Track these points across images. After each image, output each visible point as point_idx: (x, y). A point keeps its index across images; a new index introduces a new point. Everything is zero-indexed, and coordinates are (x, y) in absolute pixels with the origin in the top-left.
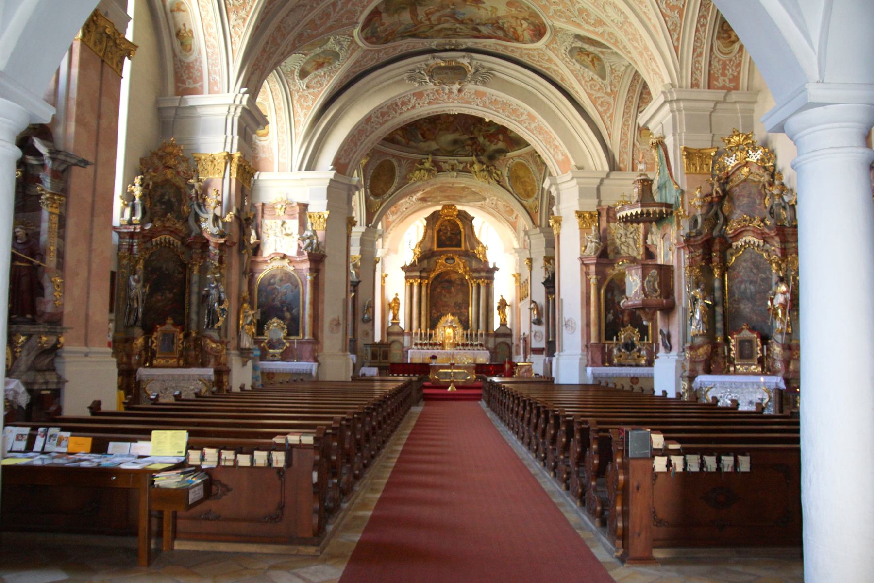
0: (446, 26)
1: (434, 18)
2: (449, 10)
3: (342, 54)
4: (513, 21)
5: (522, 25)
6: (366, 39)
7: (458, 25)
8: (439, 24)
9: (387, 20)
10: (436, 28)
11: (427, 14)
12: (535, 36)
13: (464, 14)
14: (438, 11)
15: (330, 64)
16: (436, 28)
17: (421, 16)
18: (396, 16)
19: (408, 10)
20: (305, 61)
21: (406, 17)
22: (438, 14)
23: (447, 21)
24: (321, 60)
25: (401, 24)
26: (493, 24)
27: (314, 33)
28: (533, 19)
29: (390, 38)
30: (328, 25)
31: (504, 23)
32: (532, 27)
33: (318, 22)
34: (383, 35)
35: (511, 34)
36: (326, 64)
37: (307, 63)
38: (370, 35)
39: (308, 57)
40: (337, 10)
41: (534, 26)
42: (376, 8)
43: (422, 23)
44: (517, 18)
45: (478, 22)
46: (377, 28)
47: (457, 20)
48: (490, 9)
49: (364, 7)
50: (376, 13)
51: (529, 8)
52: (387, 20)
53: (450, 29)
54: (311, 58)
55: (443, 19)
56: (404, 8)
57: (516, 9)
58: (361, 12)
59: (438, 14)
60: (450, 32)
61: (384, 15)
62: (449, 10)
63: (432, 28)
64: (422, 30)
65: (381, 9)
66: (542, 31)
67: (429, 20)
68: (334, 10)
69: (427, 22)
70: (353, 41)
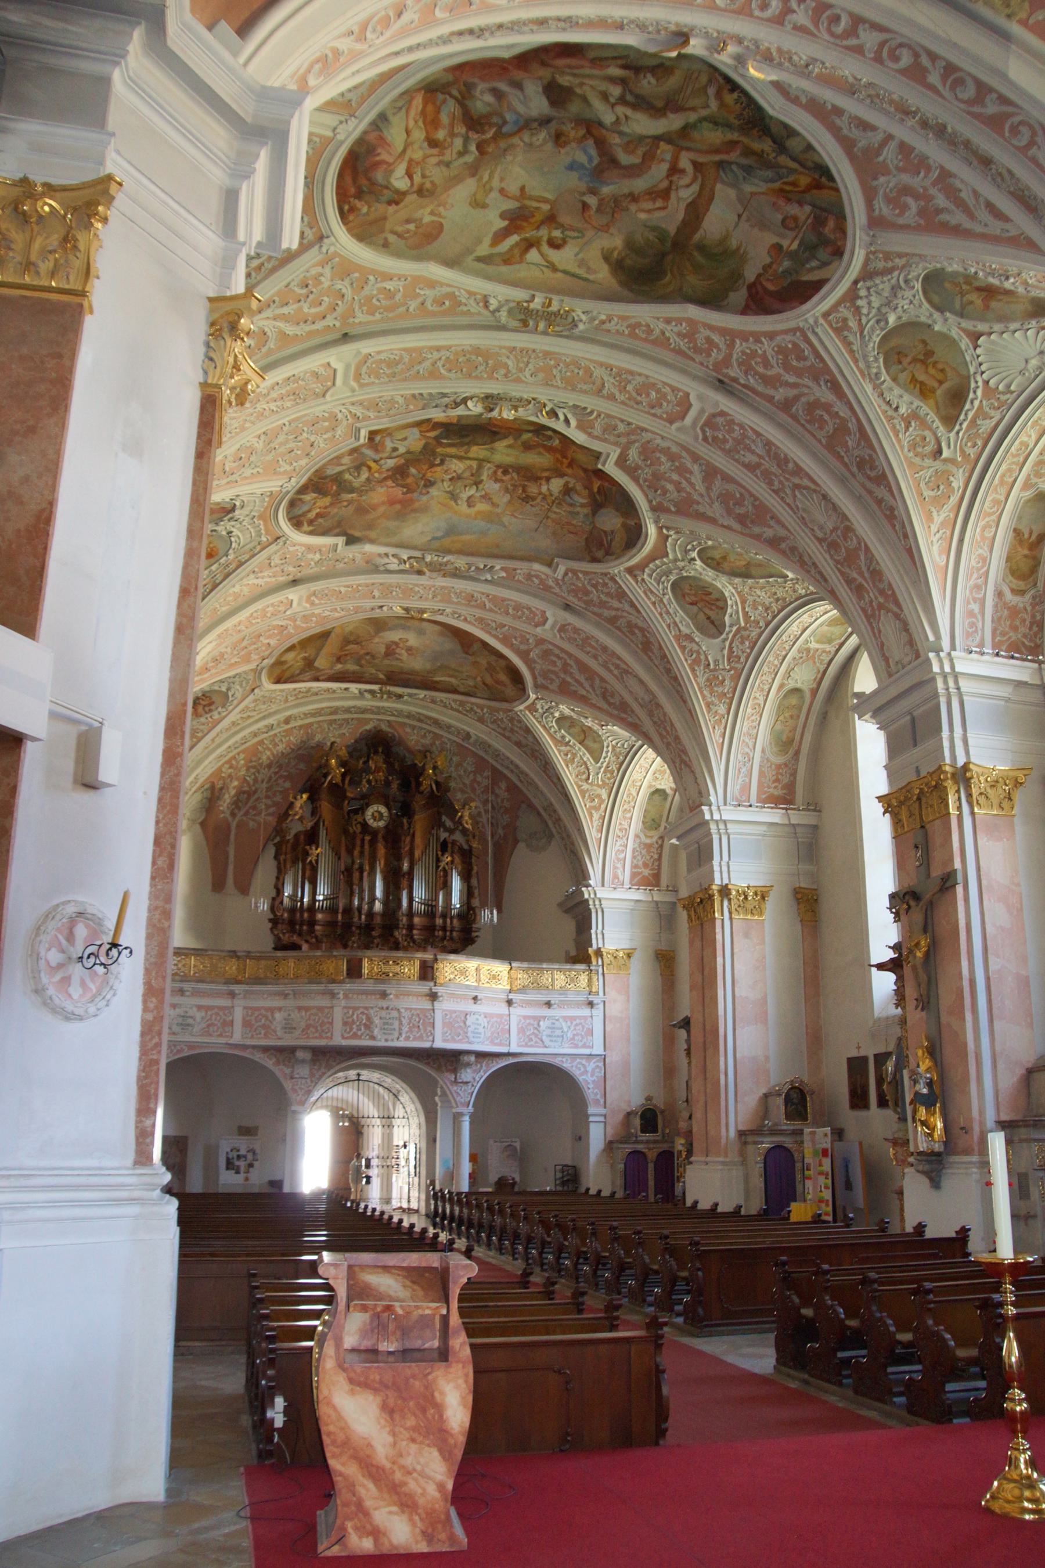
0: (643, 125)
1: (658, 171)
2: (606, 190)
3: (919, 271)
4: (437, 174)
5: (409, 175)
6: (839, 253)
7: (608, 118)
8: (657, 138)
9: (758, 250)
10: (673, 122)
11: (665, 194)
12: (371, 150)
13: (572, 167)
14: (634, 198)
15: (969, 279)
16: (673, 122)
17: (686, 193)
18: (734, 243)
19: (697, 237)
20: (997, 327)
21: (719, 220)
22: (640, 184)
23: (633, 143)
24: (975, 298)
25: (746, 202)
26: (498, 136)
27: (852, 425)
28: (380, 208)
29: (804, 181)
30: (826, 395)
31: (461, 154)
32: (379, 176)
33: (830, 428)
34: (802, 213)
35: (449, 109)
36: (977, 284)
37: (1003, 318)
38: (823, 254)
39: (981, 327)
40: (795, 392)
41: (373, 183)
42: (744, 311)
43: (696, 165)
44: (420, 192)
45: (543, 135)
46: (792, 255)
47: (601, 144)
48: (494, 194)
49: (757, 337)
50: (759, 301)
51: (386, 245)
52: (758, 250)
53: (642, 104)
54: (983, 319)
55: (635, 159)
56: (701, 248)
57: (418, 222)
58: (771, 336)
59: (640, 184)
60: (647, 84)
61: (750, 274)
62: (606, 190)
63: (685, 131)
64: (715, 136)
65: (739, 296)
66: (348, 179)
67: (674, 170)
68: (796, 398)
69: (685, 162)
70: (867, 274)
